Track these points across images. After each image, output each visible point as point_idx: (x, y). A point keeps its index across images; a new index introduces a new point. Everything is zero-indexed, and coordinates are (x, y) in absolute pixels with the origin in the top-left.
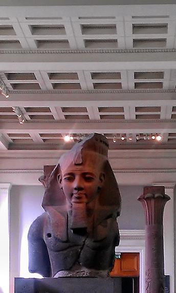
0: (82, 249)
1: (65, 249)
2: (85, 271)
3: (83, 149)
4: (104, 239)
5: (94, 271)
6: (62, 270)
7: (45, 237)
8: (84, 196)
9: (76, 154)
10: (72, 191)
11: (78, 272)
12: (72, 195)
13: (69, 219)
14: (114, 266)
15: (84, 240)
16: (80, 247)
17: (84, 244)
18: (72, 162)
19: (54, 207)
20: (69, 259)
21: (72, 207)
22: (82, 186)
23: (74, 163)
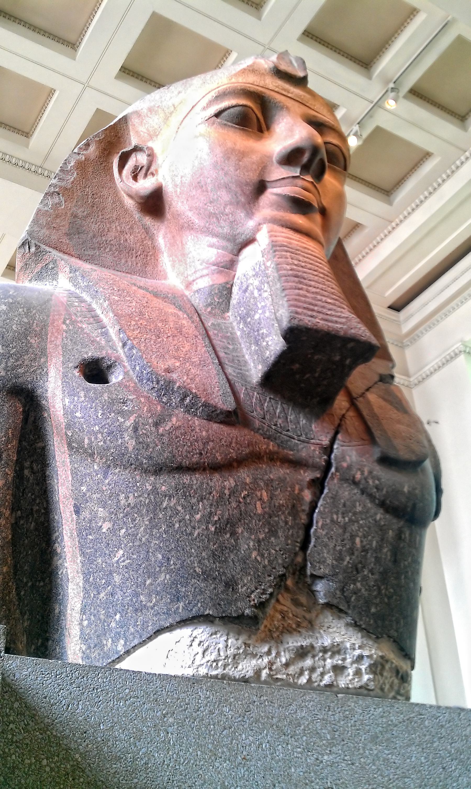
0: (318, 485)
6: (183, 623)
11: (302, 653)
12: (261, 187)
13: (209, 324)
15: (326, 441)
17: (329, 465)
21: (230, 266)
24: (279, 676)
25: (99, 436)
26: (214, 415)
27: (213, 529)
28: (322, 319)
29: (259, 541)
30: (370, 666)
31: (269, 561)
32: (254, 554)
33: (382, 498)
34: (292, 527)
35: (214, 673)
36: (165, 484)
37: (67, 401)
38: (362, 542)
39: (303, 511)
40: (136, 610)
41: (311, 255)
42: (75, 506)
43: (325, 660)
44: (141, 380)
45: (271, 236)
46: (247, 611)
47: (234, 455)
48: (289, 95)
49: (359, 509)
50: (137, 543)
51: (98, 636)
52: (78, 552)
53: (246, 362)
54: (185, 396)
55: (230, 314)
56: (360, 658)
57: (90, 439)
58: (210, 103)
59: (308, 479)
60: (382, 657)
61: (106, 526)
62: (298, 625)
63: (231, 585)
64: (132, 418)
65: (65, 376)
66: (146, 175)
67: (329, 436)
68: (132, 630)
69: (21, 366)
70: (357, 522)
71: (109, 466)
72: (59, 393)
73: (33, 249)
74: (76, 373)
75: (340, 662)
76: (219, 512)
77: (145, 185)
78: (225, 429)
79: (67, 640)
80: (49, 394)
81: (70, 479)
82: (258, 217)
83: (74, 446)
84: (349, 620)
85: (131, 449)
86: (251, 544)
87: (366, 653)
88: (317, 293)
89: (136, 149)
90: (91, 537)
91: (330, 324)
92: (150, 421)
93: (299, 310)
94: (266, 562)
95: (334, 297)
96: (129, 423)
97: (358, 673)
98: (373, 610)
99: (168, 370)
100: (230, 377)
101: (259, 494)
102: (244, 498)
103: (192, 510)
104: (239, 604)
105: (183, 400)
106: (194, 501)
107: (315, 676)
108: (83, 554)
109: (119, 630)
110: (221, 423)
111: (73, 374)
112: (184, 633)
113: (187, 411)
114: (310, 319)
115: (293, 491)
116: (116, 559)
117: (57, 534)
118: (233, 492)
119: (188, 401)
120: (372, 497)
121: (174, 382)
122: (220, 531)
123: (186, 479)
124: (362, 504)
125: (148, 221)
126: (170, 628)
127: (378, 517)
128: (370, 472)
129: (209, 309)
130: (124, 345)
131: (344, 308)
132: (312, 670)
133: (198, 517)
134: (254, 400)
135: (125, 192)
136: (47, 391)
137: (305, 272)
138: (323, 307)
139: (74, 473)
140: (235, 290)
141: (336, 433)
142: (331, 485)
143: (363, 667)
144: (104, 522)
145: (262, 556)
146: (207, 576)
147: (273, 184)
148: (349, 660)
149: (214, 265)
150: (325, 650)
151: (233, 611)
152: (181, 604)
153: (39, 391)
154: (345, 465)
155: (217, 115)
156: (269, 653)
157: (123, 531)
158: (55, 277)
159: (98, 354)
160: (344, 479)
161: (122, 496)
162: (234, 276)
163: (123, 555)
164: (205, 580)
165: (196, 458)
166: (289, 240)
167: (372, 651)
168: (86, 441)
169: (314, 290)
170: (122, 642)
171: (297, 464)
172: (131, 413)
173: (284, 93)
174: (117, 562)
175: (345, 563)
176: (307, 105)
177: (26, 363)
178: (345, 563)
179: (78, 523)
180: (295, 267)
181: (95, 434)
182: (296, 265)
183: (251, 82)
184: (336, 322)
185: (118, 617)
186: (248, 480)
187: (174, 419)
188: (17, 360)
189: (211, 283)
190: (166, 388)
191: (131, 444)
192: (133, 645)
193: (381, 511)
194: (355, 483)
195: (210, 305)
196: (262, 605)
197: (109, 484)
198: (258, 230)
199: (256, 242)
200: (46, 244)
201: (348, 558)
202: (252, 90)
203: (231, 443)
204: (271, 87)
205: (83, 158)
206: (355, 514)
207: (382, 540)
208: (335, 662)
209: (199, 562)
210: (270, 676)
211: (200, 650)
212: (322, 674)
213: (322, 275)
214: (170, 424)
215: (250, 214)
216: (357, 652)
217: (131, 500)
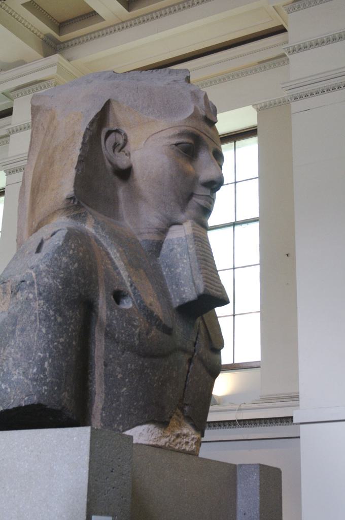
11: (178, 436)
12: (191, 195)
21: (164, 232)
25: (124, 335)
37: (109, 313)
40: (129, 414)
42: (104, 362)
43: (183, 439)
44: (140, 308)
45: (193, 229)
48: (209, 136)
50: (132, 386)
51: (110, 422)
52: (103, 383)
53: (169, 293)
55: (159, 258)
56: (193, 439)
57: (118, 335)
58: (174, 136)
61: (120, 376)
64: (138, 330)
66: (120, 151)
68: (126, 422)
71: (125, 350)
72: (105, 307)
73: (76, 203)
77: (122, 161)
79: (92, 419)
80: (99, 306)
81: (103, 349)
82: (187, 214)
83: (109, 335)
84: (192, 423)
85: (136, 344)
89: (117, 131)
90: (111, 379)
91: (218, 293)
92: (145, 332)
105: (156, 322)
106: (155, 371)
108: (106, 384)
109: (120, 421)
111: (111, 299)
112: (145, 427)
116: (122, 391)
117: (90, 371)
119: (158, 323)
125: (116, 179)
129: (150, 254)
132: (180, 443)
133: (156, 378)
135: (107, 158)
136: (98, 304)
139: (106, 348)
140: (164, 246)
141: (198, 334)
143: (193, 443)
144: (119, 374)
148: (190, 440)
149: (156, 229)
150: (184, 435)
152: (147, 415)
155: (176, 145)
156: (169, 436)
157: (127, 380)
158: (84, 221)
161: (129, 365)
162: (165, 238)
163: (126, 390)
168: (117, 336)
170: (121, 426)
174: (123, 392)
179: (105, 370)
181: (122, 334)
185: (120, 416)
187: (153, 332)
189: (152, 239)
191: (137, 342)
192: (126, 428)
195: (151, 251)
197: (124, 358)
198: (185, 221)
199: (181, 226)
200: (83, 202)
210: (169, 445)
215: (183, 210)
216: (193, 436)
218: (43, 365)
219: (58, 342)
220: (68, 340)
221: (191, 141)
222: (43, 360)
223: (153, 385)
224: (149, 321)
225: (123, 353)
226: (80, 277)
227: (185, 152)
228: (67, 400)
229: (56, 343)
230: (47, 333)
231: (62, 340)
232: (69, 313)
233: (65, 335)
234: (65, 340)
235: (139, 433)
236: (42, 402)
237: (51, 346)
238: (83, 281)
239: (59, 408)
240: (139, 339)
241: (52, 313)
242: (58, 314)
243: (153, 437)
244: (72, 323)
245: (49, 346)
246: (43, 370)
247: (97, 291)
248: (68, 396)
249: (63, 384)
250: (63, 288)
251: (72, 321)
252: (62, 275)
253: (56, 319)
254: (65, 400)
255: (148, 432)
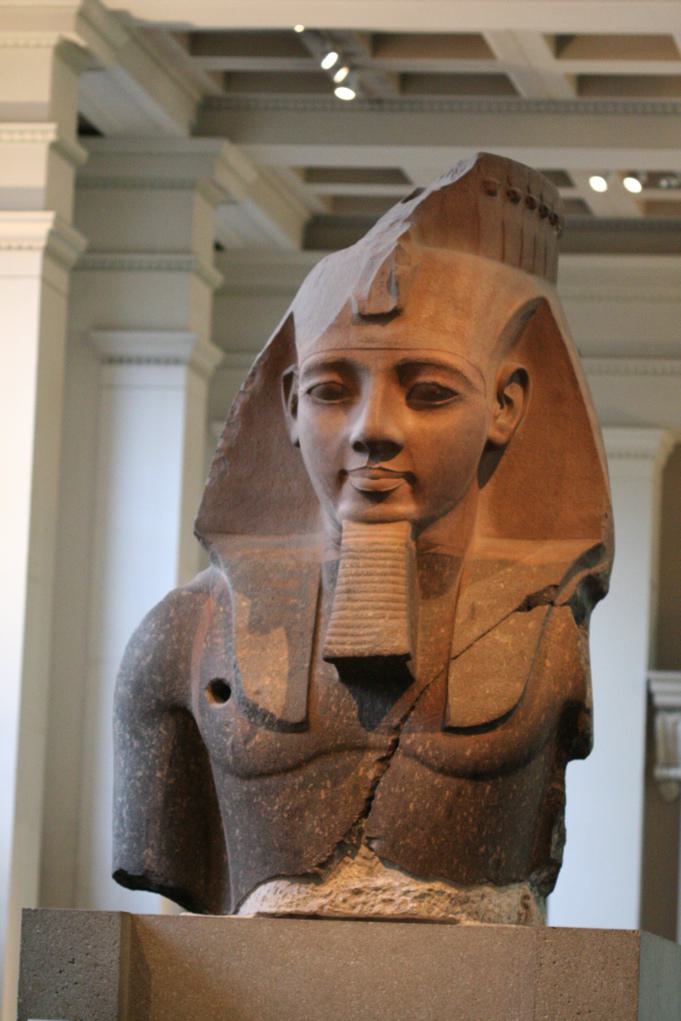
0: (384, 761)
1: (298, 766)
2: (397, 889)
3: (405, 237)
4: (504, 719)
5: (437, 886)
7: (197, 698)
8: (404, 486)
9: (373, 259)
10: (341, 454)
12: (342, 476)
14: (558, 865)
15: (396, 721)
16: (372, 756)
17: (396, 743)
18: (348, 306)
19: (254, 539)
20: (312, 824)
22: (394, 432)
23: (355, 310)
24: (336, 910)
26: (285, 727)
27: (286, 815)
28: (352, 644)
29: (321, 820)
30: (416, 898)
31: (330, 834)
32: (317, 829)
33: (440, 765)
34: (352, 804)
35: (289, 910)
36: (253, 786)
38: (415, 806)
39: (366, 788)
41: (376, 551)
43: (377, 896)
46: (309, 871)
47: (302, 758)
48: (373, 346)
49: (417, 777)
54: (265, 716)
56: (406, 893)
59: (377, 758)
60: (430, 890)
62: (359, 872)
63: (298, 853)
64: (231, 738)
65: (200, 696)
67: (402, 716)
69: (174, 690)
70: (413, 789)
74: (207, 695)
75: (389, 897)
76: (291, 803)
78: (295, 738)
86: (315, 823)
87: (412, 888)
88: (360, 609)
91: (357, 647)
92: (241, 740)
93: (333, 639)
94: (326, 834)
95: (381, 604)
96: (229, 743)
97: (404, 902)
98: (421, 857)
99: (258, 693)
100: (316, 679)
101: (323, 784)
102: (311, 789)
103: (272, 803)
104: (304, 866)
105: (264, 719)
106: (272, 797)
107: (365, 907)
110: (295, 732)
112: (271, 885)
113: (267, 728)
114: (340, 647)
115: (357, 773)
118: (303, 786)
119: (267, 720)
120: (430, 766)
121: (258, 705)
122: (292, 816)
123: (267, 782)
124: (421, 774)
126: (264, 882)
127: (436, 782)
128: (432, 744)
130: (235, 666)
131: (384, 617)
132: (364, 903)
133: (276, 808)
134: (332, 699)
137: (359, 582)
138: (358, 627)
142: (398, 760)
143: (409, 899)
145: (323, 830)
146: (282, 849)
147: (353, 473)
151: (298, 871)
152: (268, 868)
153: (189, 708)
154: (408, 742)
155: (309, 391)
156: (331, 893)
159: (221, 676)
160: (406, 755)
164: (281, 852)
165: (272, 767)
166: (357, 539)
167: (423, 887)
169: (360, 604)
171: (364, 748)
172: (230, 733)
173: (368, 346)
175: (397, 825)
176: (397, 347)
177: (178, 686)
178: (397, 825)
180: (351, 578)
182: (353, 575)
183: (333, 347)
184: (365, 643)
186: (314, 775)
188: (171, 686)
190: (253, 711)
191: (231, 758)
193: (441, 776)
194: (416, 757)
196: (322, 865)
201: (400, 821)
202: (331, 361)
203: (299, 748)
204: (355, 344)
205: (248, 396)
206: (411, 783)
207: (437, 800)
208: (385, 896)
209: (278, 840)
211: (281, 896)
212: (373, 906)
213: (376, 579)
214: (253, 742)
215: (336, 505)
216: (405, 889)
217: (239, 798)
218: (121, 814)
219: (135, 778)
220: (147, 773)
221: (334, 377)
222: (122, 804)
223: (272, 820)
224: (252, 720)
225: (224, 778)
226: (155, 674)
227: (325, 399)
228: (153, 860)
229: (132, 781)
230: (125, 767)
231: (140, 774)
232: (147, 732)
233: (143, 767)
234: (144, 773)
235: (262, 895)
236: (125, 869)
237: (128, 786)
238: (159, 679)
239: (139, 874)
240: (233, 753)
241: (128, 736)
242: (133, 737)
243: (287, 900)
244: (152, 746)
245: (126, 787)
246: (122, 820)
247: (188, 688)
248: (155, 854)
249: (143, 839)
250: (134, 697)
251: (153, 743)
252: (132, 679)
253: (132, 745)
254: (148, 861)
255: (275, 893)
